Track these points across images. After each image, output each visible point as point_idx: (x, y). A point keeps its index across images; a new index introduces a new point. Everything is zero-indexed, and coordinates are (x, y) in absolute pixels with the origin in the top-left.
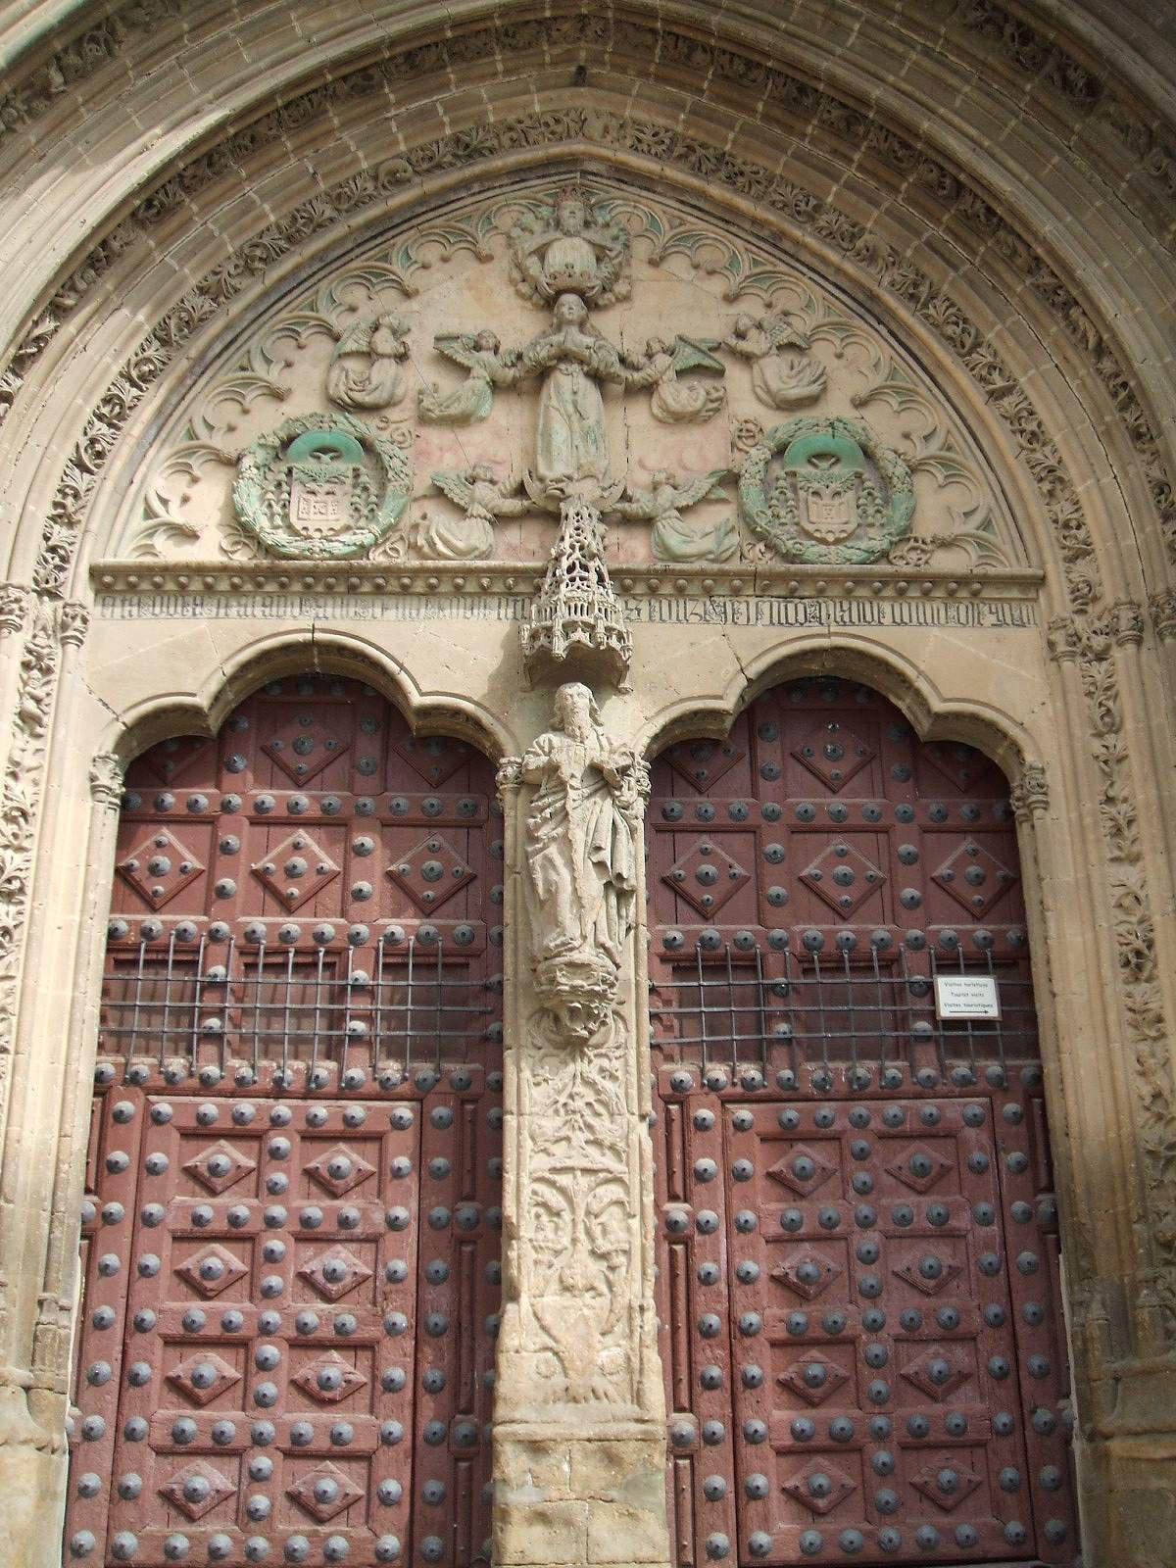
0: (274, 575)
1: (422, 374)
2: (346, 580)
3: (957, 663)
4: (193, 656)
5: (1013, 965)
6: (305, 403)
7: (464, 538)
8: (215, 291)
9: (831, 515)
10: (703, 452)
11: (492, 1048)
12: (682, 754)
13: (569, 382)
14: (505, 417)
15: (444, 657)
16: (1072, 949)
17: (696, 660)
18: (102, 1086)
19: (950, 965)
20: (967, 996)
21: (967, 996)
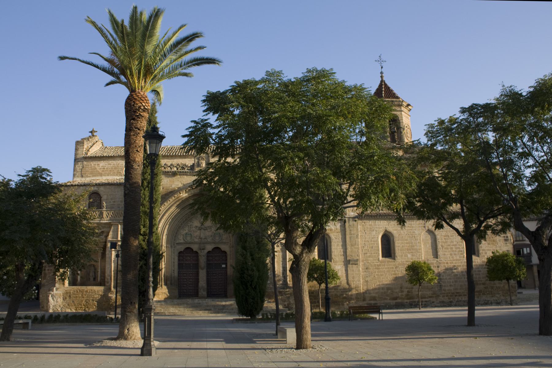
0: (186, 243)
1: (194, 229)
2: (190, 243)
3: (224, 247)
4: (182, 248)
5: (226, 264)
6: (187, 231)
7: (196, 240)
8: (181, 224)
9: (217, 238)
10: (210, 234)
11: (198, 269)
12: (209, 252)
13: (202, 230)
14: (199, 231)
15: (195, 248)
16: (229, 264)
17: (209, 248)
18: (179, 272)
19: (223, 264)
20: (224, 266)
21: (224, 266)
